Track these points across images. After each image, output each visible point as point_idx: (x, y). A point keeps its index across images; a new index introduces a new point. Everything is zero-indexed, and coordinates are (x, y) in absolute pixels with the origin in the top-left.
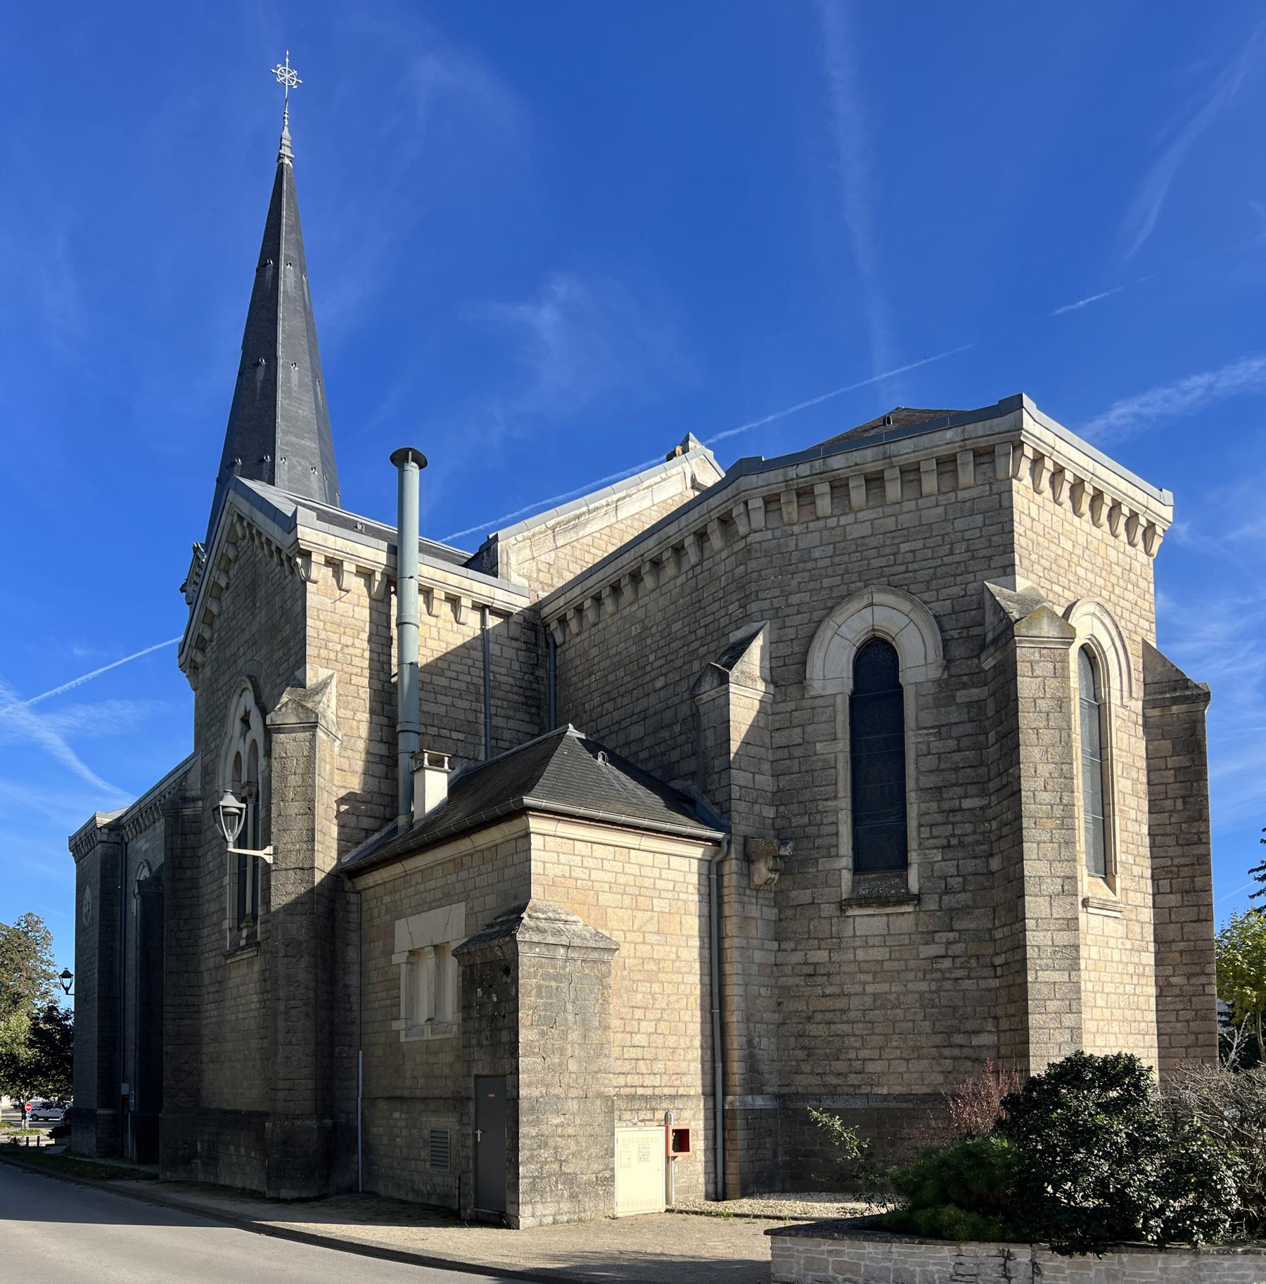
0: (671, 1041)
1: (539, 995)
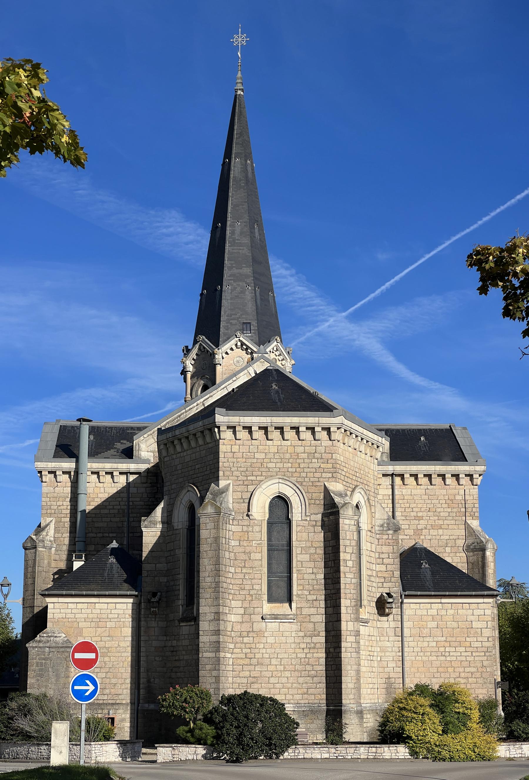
0: (114, 681)
1: (37, 666)
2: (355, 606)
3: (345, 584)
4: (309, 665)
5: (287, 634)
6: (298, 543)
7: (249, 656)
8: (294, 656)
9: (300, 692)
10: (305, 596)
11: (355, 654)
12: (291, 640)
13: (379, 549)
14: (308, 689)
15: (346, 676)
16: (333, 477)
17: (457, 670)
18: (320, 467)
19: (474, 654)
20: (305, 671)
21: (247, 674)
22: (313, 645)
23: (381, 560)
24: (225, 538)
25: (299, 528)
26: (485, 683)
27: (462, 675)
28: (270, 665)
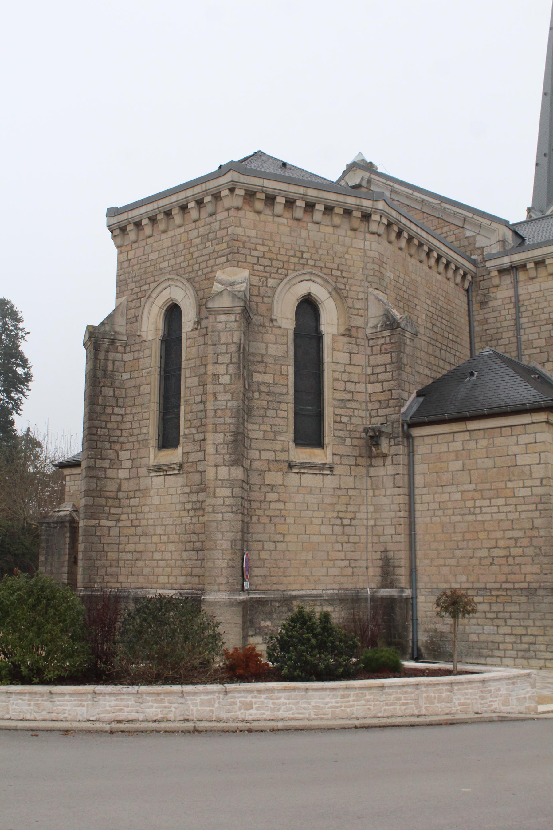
2: (232, 442)
3: (215, 410)
4: (194, 533)
5: (172, 491)
6: (187, 362)
7: (136, 523)
8: (178, 521)
9: (184, 572)
10: (192, 436)
11: (231, 515)
12: (176, 499)
13: (374, 360)
14: (192, 568)
15: (211, 549)
16: (228, 260)
17: (493, 535)
18: (214, 251)
19: (519, 508)
20: (190, 542)
21: (131, 547)
22: (198, 505)
23: (375, 376)
24: (105, 371)
25: (189, 341)
26: (537, 555)
27: (501, 543)
28: (155, 535)
